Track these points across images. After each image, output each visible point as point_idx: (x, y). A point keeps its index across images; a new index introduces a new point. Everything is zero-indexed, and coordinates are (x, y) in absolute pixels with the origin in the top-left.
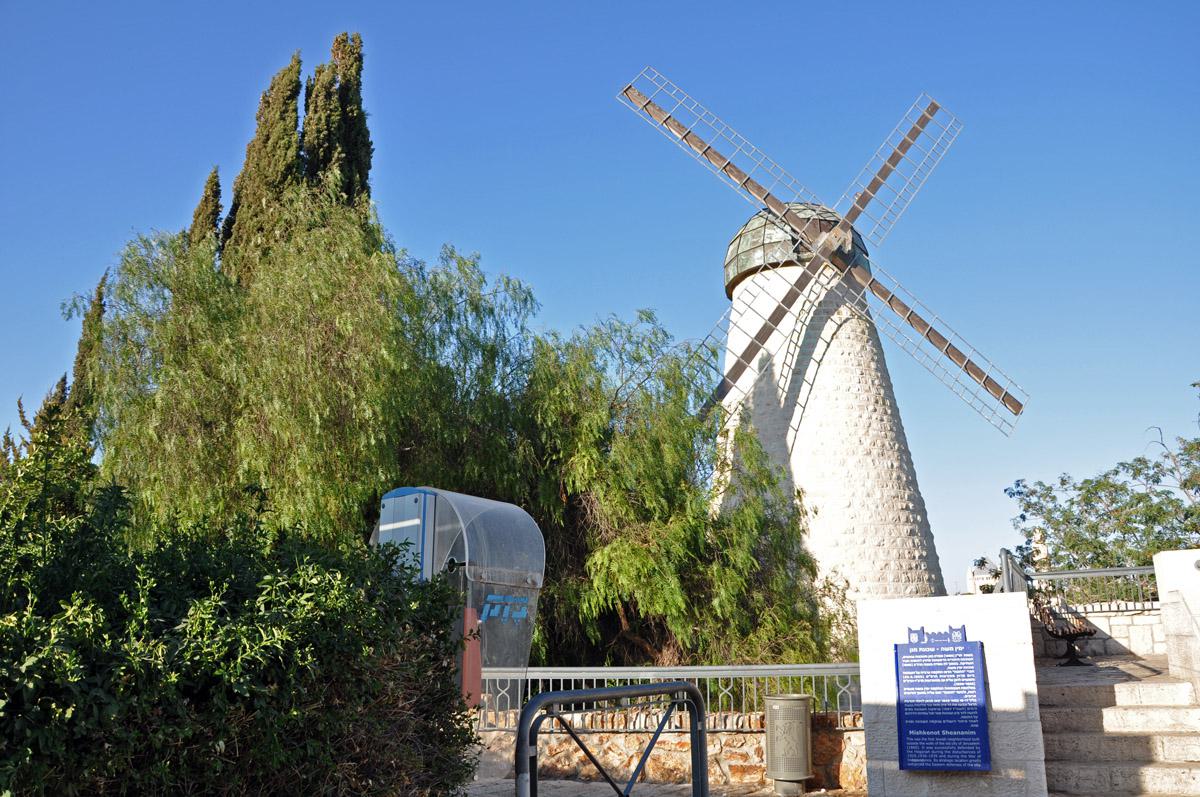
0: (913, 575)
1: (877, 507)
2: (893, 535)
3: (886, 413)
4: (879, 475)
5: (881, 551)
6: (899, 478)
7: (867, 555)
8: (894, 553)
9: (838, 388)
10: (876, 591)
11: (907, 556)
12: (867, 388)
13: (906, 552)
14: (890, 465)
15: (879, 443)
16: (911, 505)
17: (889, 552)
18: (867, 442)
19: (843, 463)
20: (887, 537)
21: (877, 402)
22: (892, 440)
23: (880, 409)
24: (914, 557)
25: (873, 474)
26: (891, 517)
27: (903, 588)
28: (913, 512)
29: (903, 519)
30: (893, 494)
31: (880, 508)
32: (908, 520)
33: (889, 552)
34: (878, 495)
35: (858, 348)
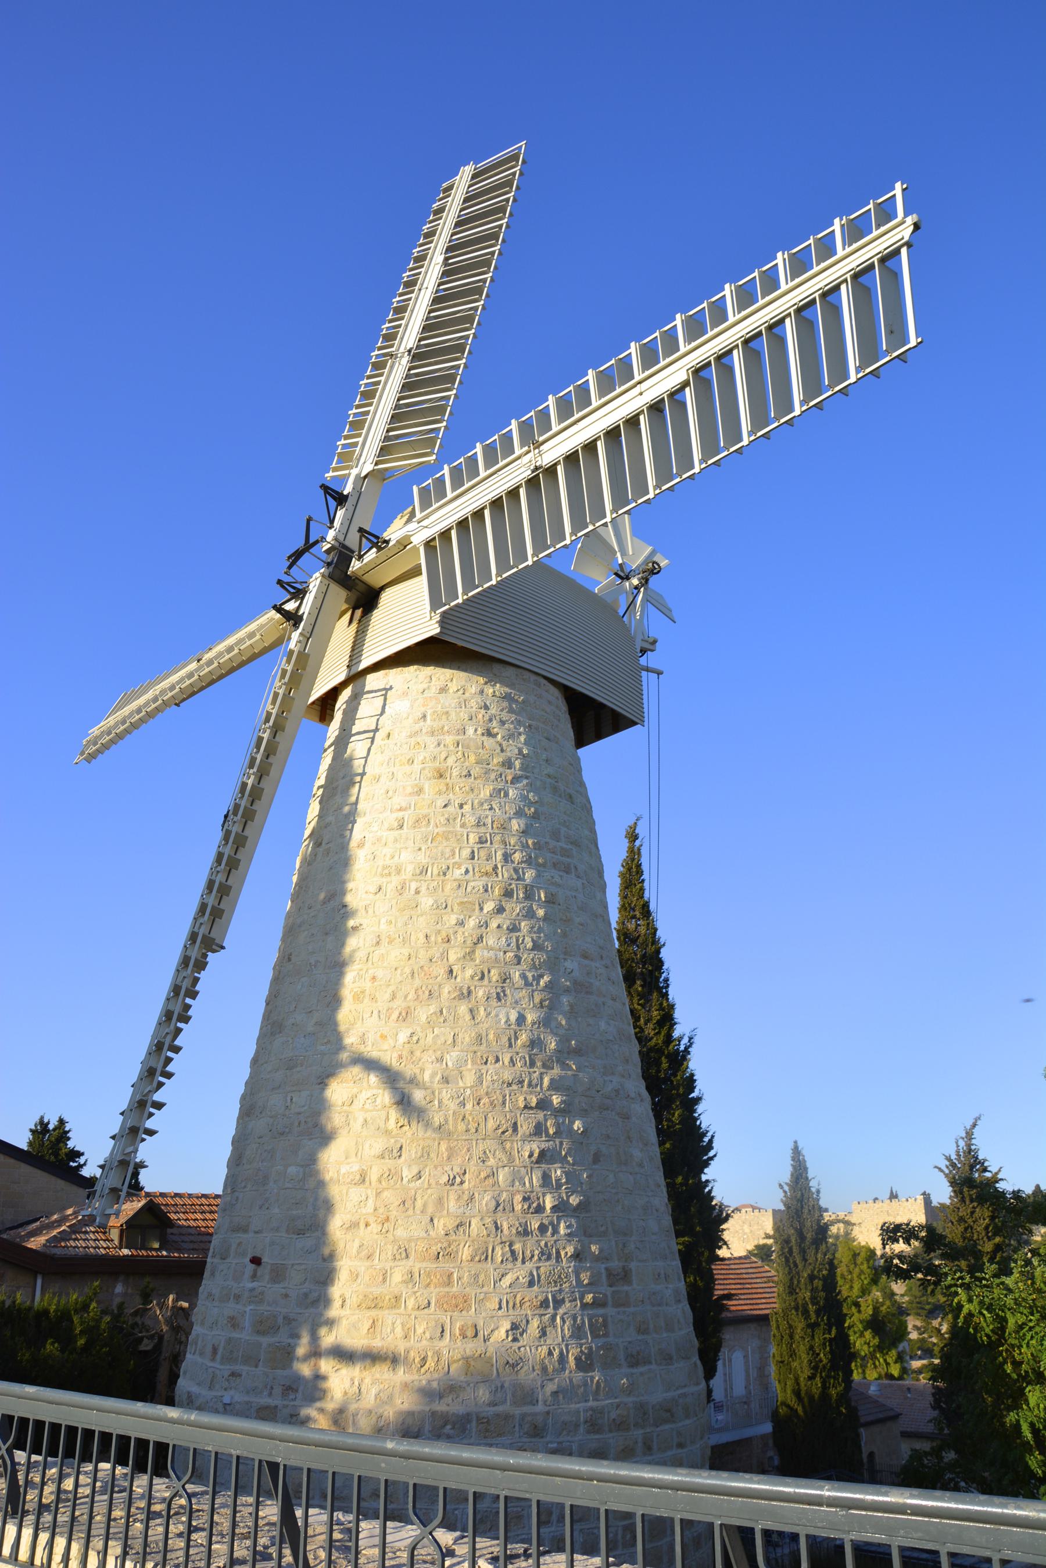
0: (532, 1245)
1: (463, 1104)
2: (492, 1162)
3: (530, 914)
4: (479, 1039)
5: (453, 1197)
6: (534, 1043)
7: (419, 1203)
8: (486, 1200)
9: (424, 871)
10: (425, 1280)
11: (518, 1207)
12: (489, 868)
13: (518, 1198)
14: (513, 1017)
15: (495, 975)
16: (556, 1100)
17: (472, 1198)
18: (466, 975)
19: (405, 1016)
20: (472, 1168)
21: (508, 894)
22: (533, 967)
23: (514, 908)
24: (540, 1209)
25: (466, 1037)
26: (491, 1124)
27: (493, 1274)
28: (558, 1112)
29: (525, 1127)
30: (507, 1075)
31: (469, 1106)
32: (539, 1130)
33: (472, 1198)
34: (470, 1079)
35: (486, 792)
